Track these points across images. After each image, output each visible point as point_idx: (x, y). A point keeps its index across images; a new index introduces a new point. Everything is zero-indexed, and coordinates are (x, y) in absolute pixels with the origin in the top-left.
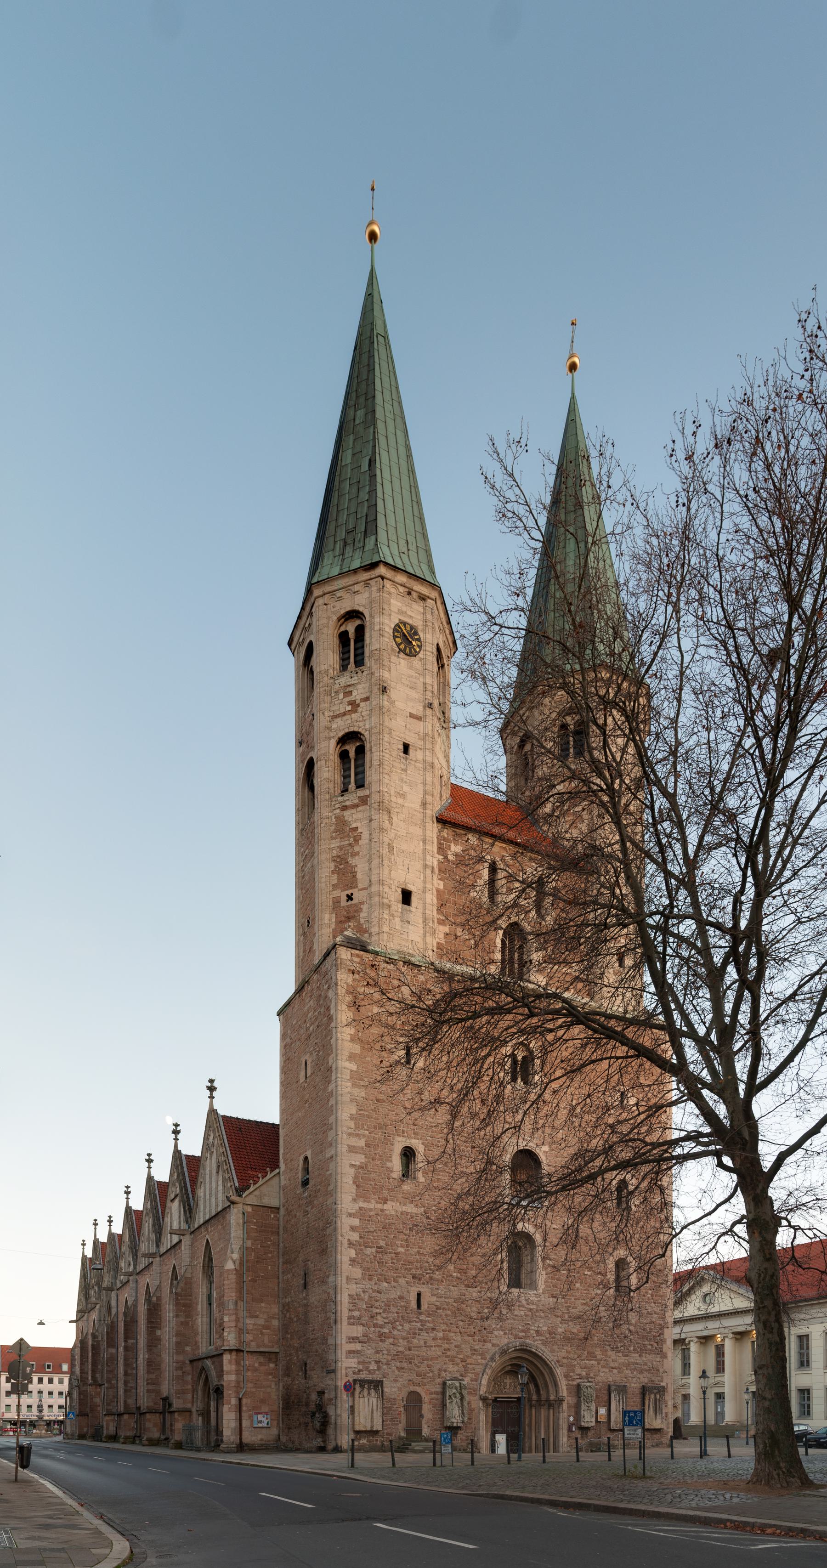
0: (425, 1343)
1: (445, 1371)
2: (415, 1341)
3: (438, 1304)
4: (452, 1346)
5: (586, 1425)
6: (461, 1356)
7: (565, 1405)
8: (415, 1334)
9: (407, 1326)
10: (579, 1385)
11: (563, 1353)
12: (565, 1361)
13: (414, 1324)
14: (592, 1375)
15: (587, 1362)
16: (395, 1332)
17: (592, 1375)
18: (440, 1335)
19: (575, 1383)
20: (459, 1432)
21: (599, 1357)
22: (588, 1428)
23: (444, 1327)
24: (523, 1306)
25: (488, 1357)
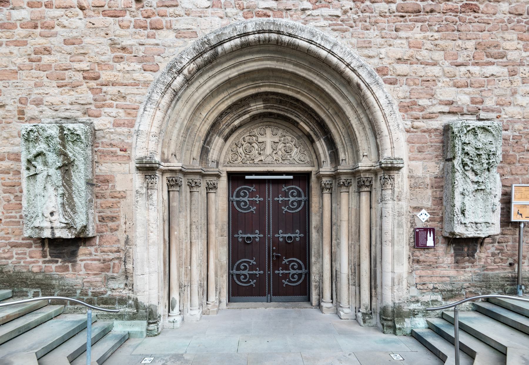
1: (38, 103)
4: (56, 42)
5: (471, 233)
6: (84, 66)
7: (401, 181)
10: (447, 129)
11: (400, 49)
12: (402, 68)
14: (489, 103)
15: (475, 69)
17: (489, 103)
19: (438, 123)
20: (83, 250)
21: (513, 55)
22: (475, 242)
25: (163, 67)
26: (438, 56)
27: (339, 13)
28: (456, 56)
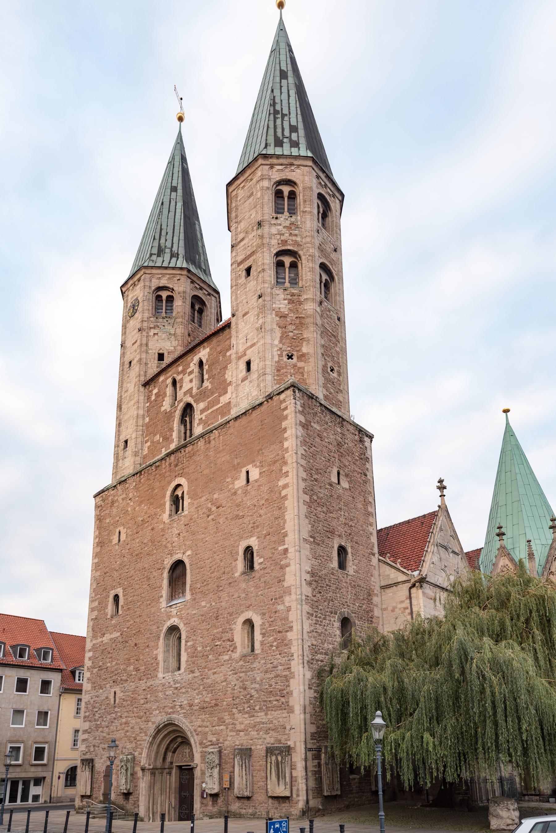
0: (117, 728)
2: (112, 727)
3: (123, 697)
8: (112, 722)
9: (109, 717)
13: (112, 715)
16: (103, 723)
18: (124, 720)
23: (126, 714)
24: (171, 687)
26: (208, 724)
27: (185, 711)
28: (213, 723)
